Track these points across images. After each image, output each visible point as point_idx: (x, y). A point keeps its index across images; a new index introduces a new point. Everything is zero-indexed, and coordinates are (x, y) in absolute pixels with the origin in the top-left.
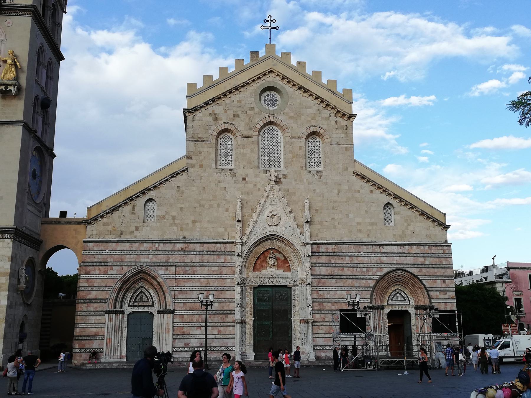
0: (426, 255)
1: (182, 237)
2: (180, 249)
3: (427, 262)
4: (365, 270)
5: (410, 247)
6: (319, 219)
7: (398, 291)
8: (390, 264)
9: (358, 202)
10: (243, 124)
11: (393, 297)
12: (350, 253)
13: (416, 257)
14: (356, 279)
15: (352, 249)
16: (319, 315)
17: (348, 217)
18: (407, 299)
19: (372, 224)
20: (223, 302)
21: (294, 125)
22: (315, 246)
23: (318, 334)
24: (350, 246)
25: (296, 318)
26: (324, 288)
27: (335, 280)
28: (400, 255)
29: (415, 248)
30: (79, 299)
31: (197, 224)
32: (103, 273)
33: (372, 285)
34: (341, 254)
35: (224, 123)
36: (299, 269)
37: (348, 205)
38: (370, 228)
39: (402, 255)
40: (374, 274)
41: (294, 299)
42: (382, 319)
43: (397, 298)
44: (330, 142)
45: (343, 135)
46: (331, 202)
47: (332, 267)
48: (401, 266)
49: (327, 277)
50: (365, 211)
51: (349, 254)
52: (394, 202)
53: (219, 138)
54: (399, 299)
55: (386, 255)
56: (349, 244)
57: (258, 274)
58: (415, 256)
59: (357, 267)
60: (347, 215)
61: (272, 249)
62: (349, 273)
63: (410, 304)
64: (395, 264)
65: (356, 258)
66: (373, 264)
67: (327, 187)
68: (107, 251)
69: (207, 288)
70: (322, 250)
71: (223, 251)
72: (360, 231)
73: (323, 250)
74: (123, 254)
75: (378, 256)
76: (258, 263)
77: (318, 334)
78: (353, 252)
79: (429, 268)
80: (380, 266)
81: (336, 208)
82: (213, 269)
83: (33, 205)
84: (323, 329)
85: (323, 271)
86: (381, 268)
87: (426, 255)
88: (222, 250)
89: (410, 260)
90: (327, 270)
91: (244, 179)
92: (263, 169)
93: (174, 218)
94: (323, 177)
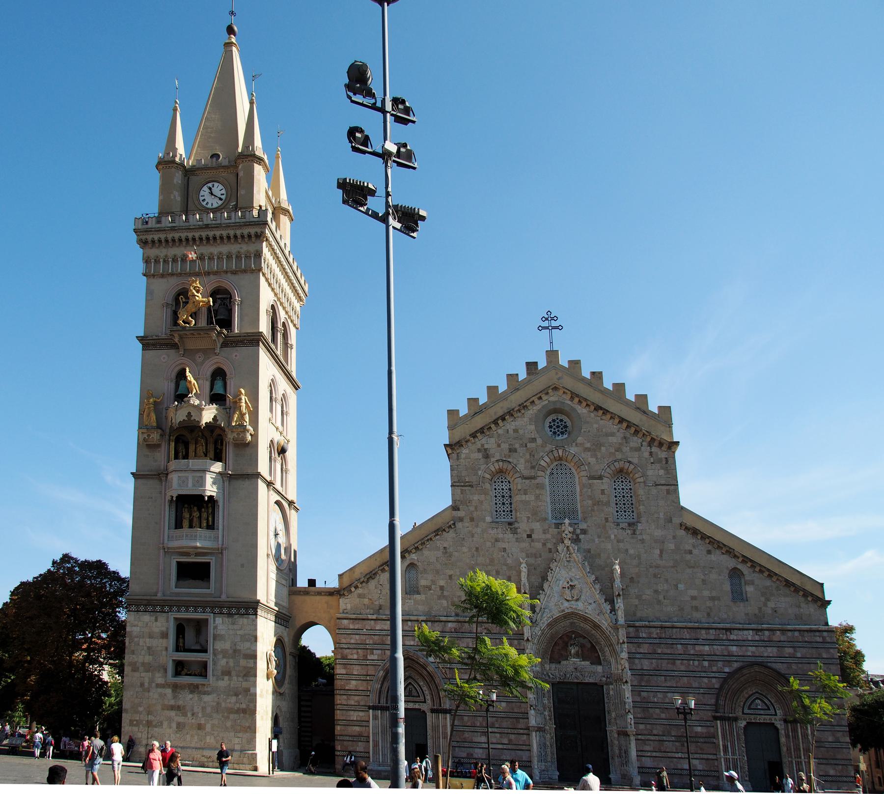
0: (796, 644)
1: (453, 614)
2: (453, 630)
3: (799, 655)
4: (706, 664)
5: (771, 633)
7: (757, 695)
8: (743, 656)
11: (750, 705)
14: (694, 676)
18: (771, 708)
24: (682, 630)
27: (663, 677)
28: (756, 644)
30: (337, 690)
32: (362, 658)
33: (717, 686)
36: (613, 661)
38: (709, 604)
39: (760, 644)
40: (719, 670)
42: (735, 735)
43: (757, 705)
47: (659, 659)
48: (760, 660)
49: (651, 673)
51: (682, 641)
52: (745, 569)
54: (759, 707)
55: (736, 643)
56: (680, 628)
58: (780, 645)
59: (694, 660)
62: (683, 668)
63: (776, 715)
64: (750, 656)
66: (717, 656)
68: (365, 630)
73: (644, 635)
74: (384, 635)
78: (688, 638)
79: (801, 663)
80: (727, 658)
85: (646, 664)
87: (796, 644)
89: (771, 651)
92: (554, 521)
93: (442, 588)
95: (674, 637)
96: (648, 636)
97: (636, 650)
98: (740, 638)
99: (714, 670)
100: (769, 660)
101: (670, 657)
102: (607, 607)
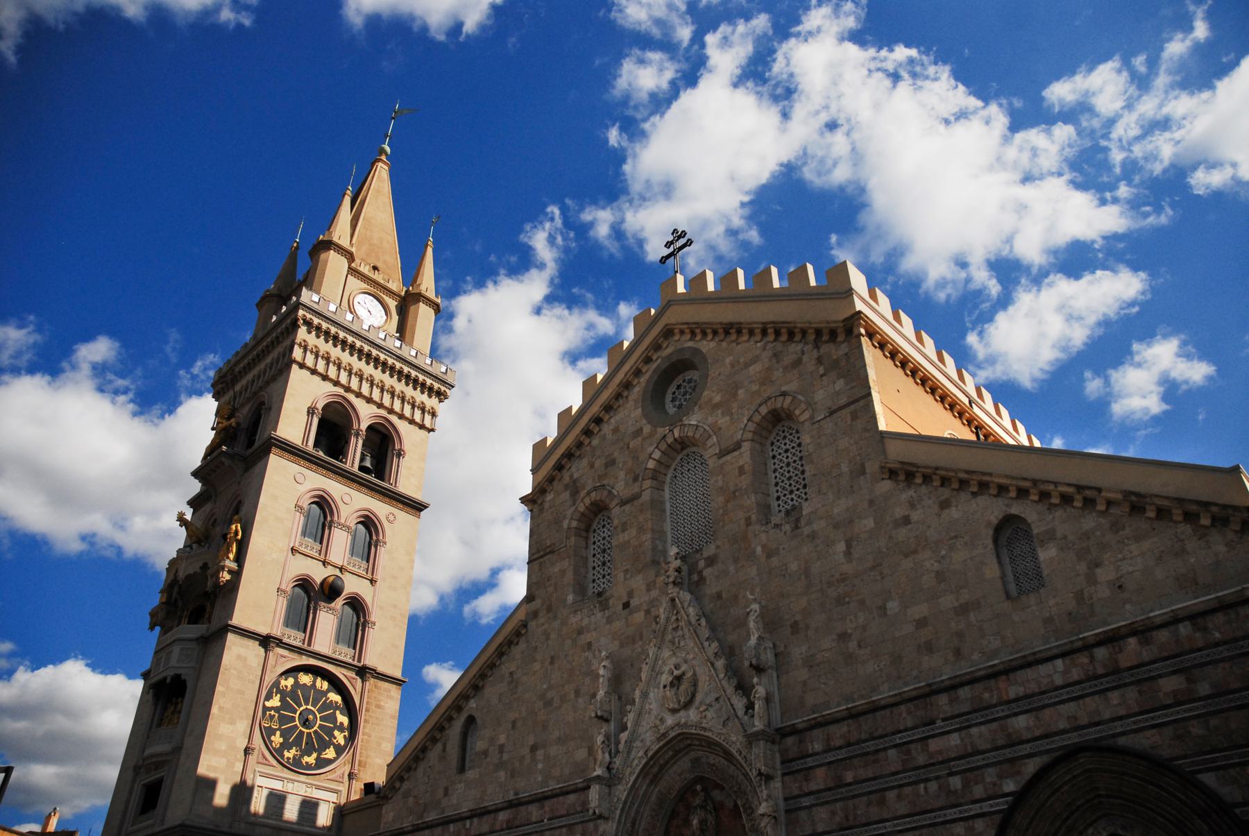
1: (512, 793)
2: (505, 826)
4: (956, 782)
6: (804, 648)
8: (1046, 736)
9: (906, 556)
10: (622, 474)
12: (900, 732)
13: (1146, 680)
15: (904, 719)
17: (885, 614)
19: (963, 610)
21: (723, 421)
22: (790, 741)
29: (1133, 646)
31: (540, 754)
34: (871, 746)
35: (589, 493)
37: (881, 574)
44: (812, 417)
45: (840, 384)
46: (830, 584)
48: (1093, 734)
50: (933, 575)
51: (898, 739)
53: (592, 530)
59: (927, 780)
60: (883, 609)
61: (700, 779)
62: (902, 809)
64: (1064, 732)
65: (919, 747)
67: (816, 546)
71: (578, 813)
72: (929, 648)
75: (995, 720)
78: (909, 724)
80: (1009, 754)
81: (847, 599)
83: (286, 778)
86: (1012, 761)
90: (834, 813)
91: (626, 605)
93: (501, 748)
94: (803, 522)
95: (880, 732)
97: (800, 788)
98: (1033, 688)
99: (978, 797)
100: (1118, 727)
101: (874, 786)
102: (739, 703)
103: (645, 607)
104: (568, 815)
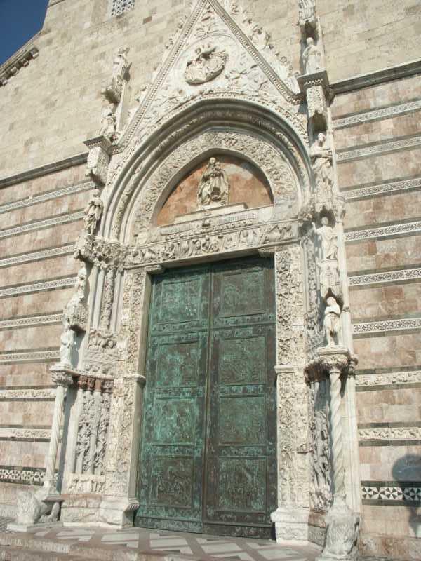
16: (385, 339)
20: (48, 324)
23: (386, 425)
25: (293, 365)
26: (402, 229)
31: (34, 146)
41: (283, 291)
57: (164, 230)
69: (19, 290)
70: (375, 104)
76: (174, 203)
77: (386, 425)
82: (40, 235)
84: (409, 401)
88: (69, 183)
96: (394, 101)
103: (168, 18)
104: (57, 189)
